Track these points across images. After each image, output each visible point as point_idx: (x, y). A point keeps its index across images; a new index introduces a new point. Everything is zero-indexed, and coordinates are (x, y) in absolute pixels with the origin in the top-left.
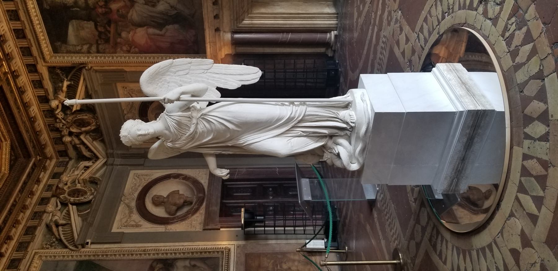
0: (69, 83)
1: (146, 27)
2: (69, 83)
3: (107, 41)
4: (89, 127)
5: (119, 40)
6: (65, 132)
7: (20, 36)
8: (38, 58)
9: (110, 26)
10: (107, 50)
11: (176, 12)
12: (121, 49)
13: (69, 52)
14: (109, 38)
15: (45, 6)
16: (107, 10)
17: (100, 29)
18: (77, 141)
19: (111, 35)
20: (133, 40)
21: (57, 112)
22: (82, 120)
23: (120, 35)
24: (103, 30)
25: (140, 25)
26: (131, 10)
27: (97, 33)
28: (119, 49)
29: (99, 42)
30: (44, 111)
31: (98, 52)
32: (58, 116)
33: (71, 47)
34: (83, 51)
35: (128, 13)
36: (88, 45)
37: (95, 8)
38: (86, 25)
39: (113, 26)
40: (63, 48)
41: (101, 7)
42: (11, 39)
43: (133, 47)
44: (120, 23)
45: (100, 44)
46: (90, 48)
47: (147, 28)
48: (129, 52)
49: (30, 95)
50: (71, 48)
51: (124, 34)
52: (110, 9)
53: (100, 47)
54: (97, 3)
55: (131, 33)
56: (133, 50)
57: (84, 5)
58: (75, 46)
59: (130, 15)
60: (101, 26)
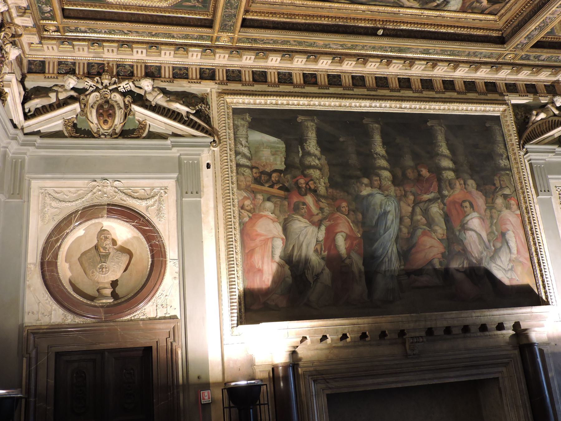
0: (184, 114)
1: (284, 237)
2: (184, 114)
3: (257, 181)
4: (95, 120)
5: (260, 197)
6: (88, 83)
7: (256, 76)
8: (225, 87)
9: (280, 188)
10: (242, 178)
11: (311, 281)
12: (245, 198)
13: (236, 128)
14: (262, 185)
15: (300, 119)
16: (303, 190)
17: (274, 175)
18: (62, 96)
19: (266, 188)
20: (261, 216)
21: (131, 84)
22: (112, 116)
23: (269, 200)
24: (273, 179)
25: (285, 229)
26: (306, 221)
27: (268, 170)
28: (245, 195)
29: (254, 170)
30: (132, 66)
31: (238, 165)
32: (126, 82)
33: (244, 133)
34: (240, 146)
35: (302, 216)
36: (249, 155)
37: (305, 176)
38: (279, 159)
39: (282, 193)
40: (240, 122)
41: (307, 184)
42: (255, 64)
43: (251, 215)
44: (286, 203)
45: (252, 171)
46: (244, 156)
47: (282, 239)
48: (242, 207)
49: (167, 58)
50: (242, 131)
51: (269, 205)
52: (306, 195)
53: (248, 171)
54: (312, 180)
55: (273, 216)
56: (245, 213)
57: (307, 163)
58: (247, 138)
59: (299, 217)
60: (280, 177)
